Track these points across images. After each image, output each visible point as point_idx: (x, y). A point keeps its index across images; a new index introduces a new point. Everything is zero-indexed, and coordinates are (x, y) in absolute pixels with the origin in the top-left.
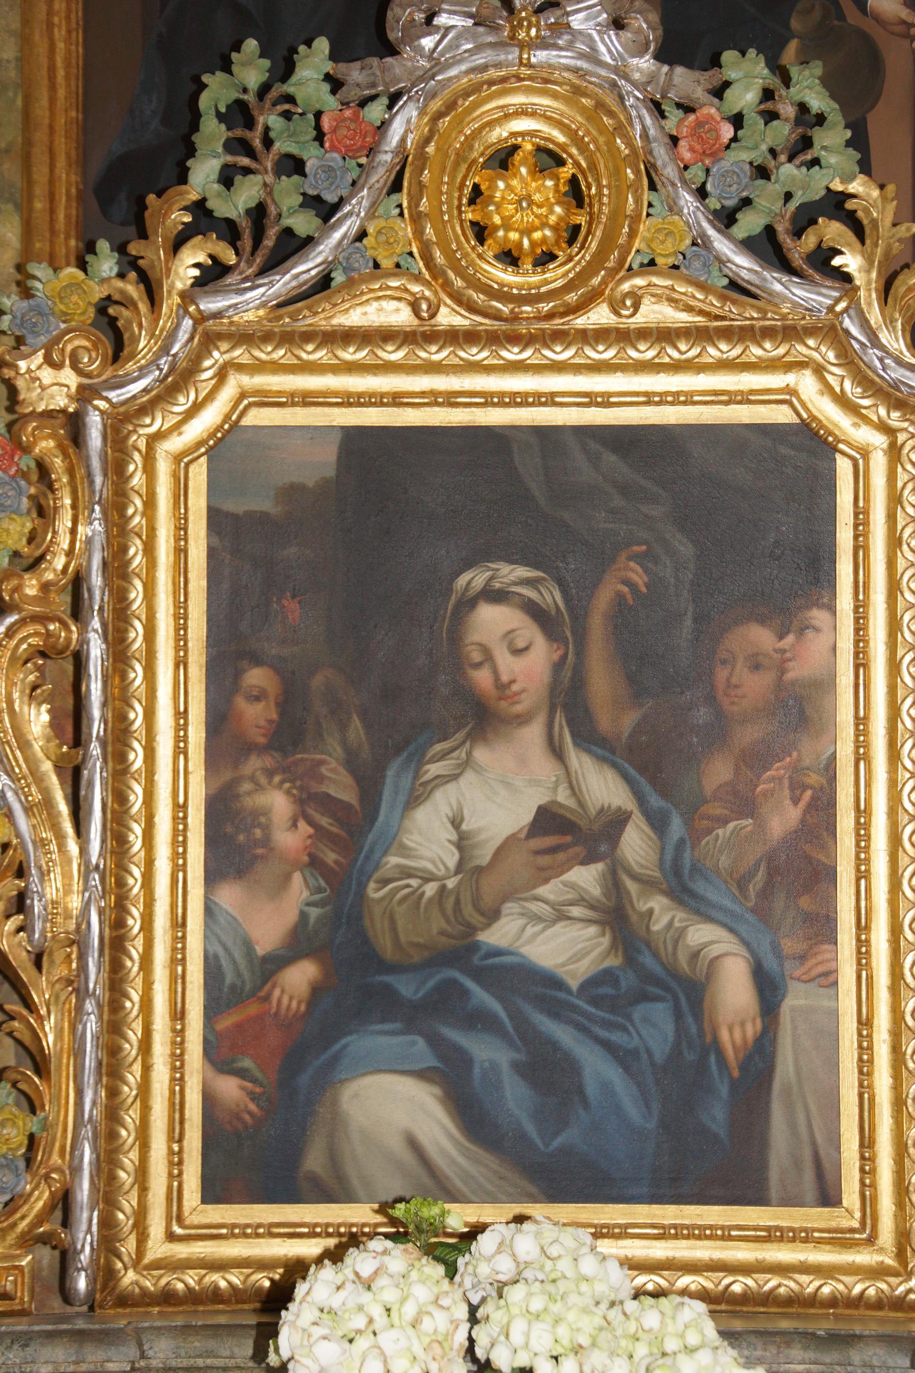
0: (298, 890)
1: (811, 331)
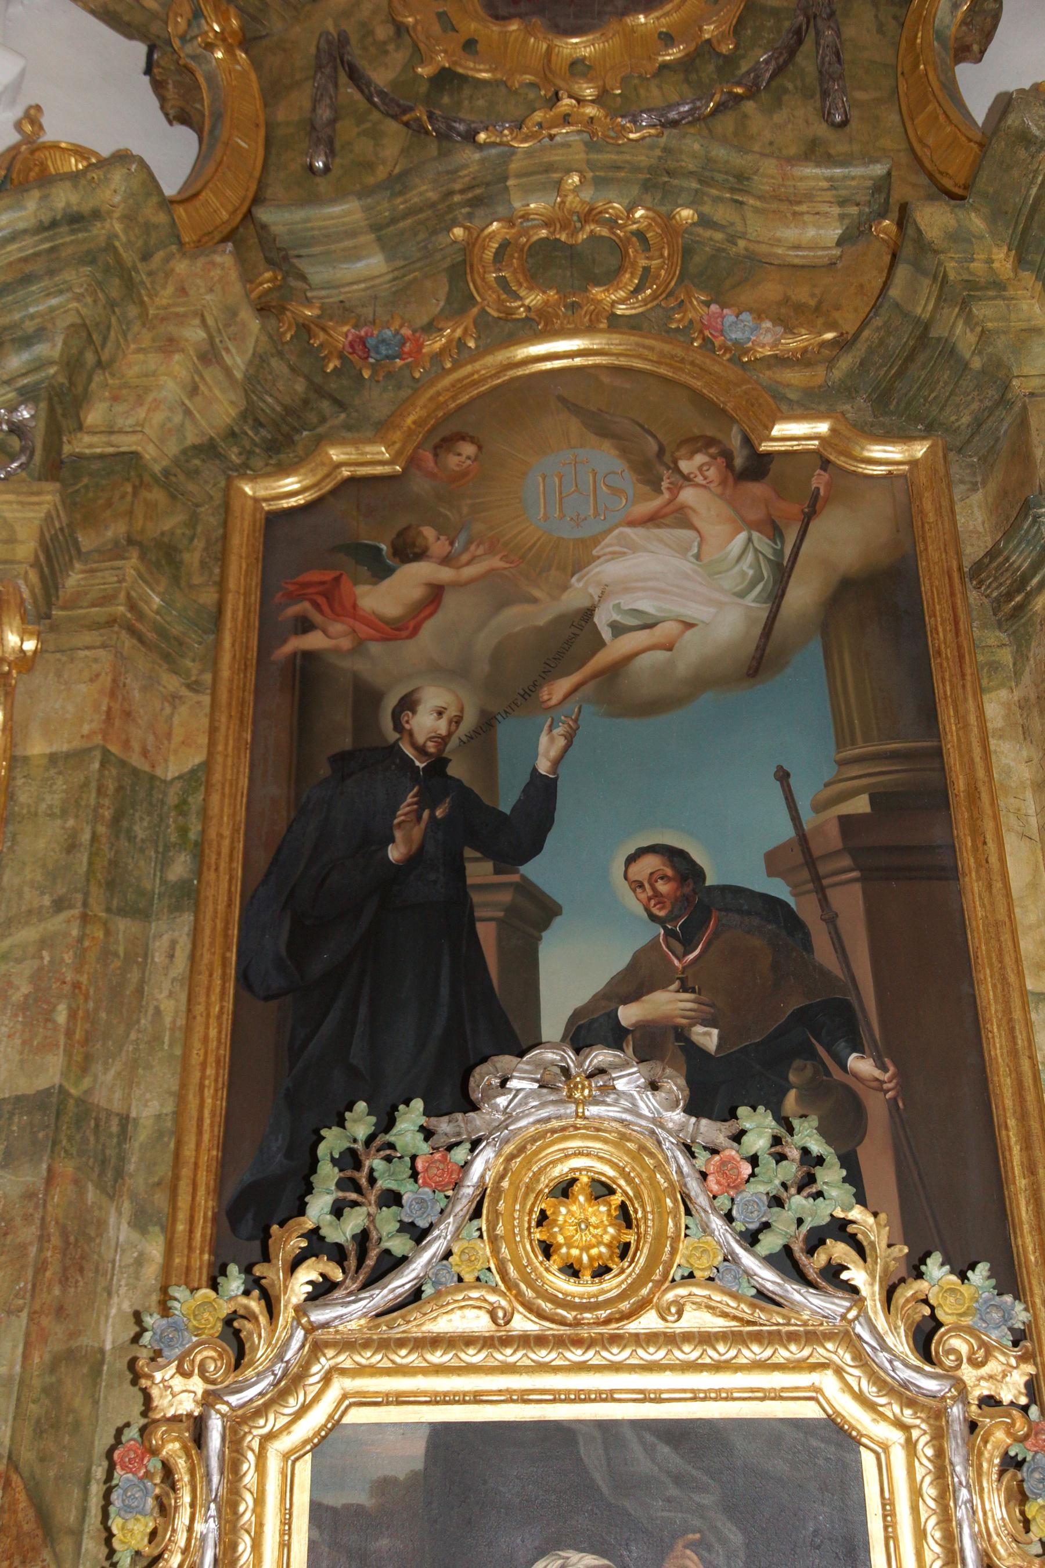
1: (829, 1336)
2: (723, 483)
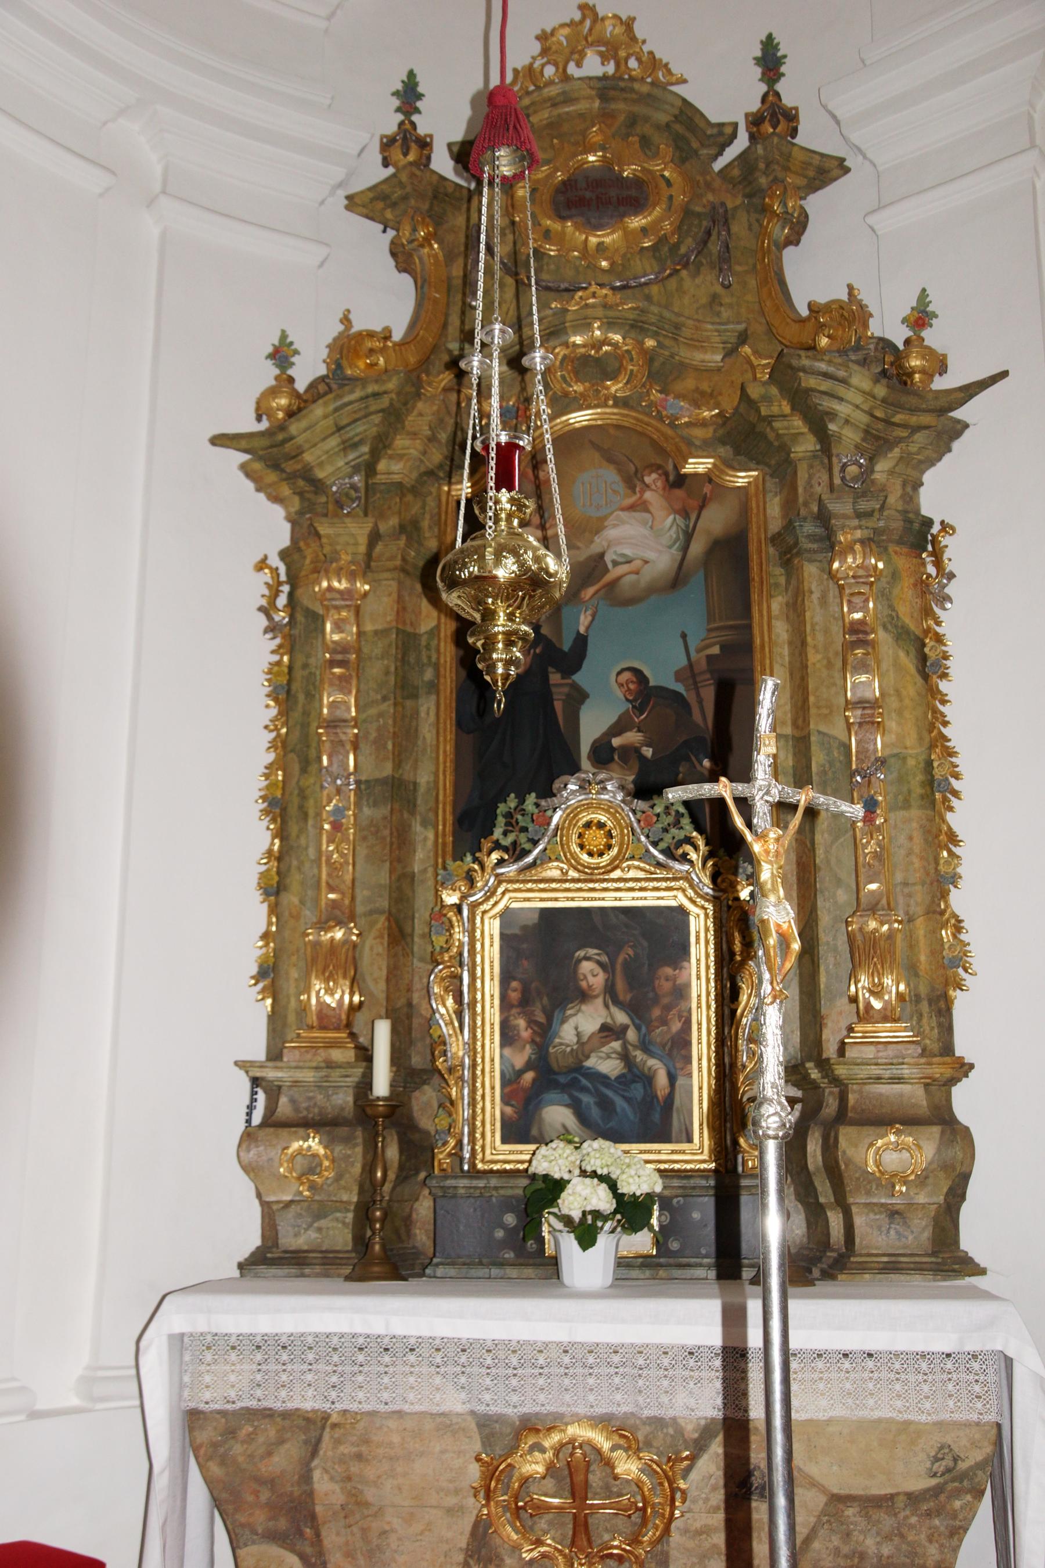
0: (528, 1050)
1: (680, 879)
2: (664, 489)
